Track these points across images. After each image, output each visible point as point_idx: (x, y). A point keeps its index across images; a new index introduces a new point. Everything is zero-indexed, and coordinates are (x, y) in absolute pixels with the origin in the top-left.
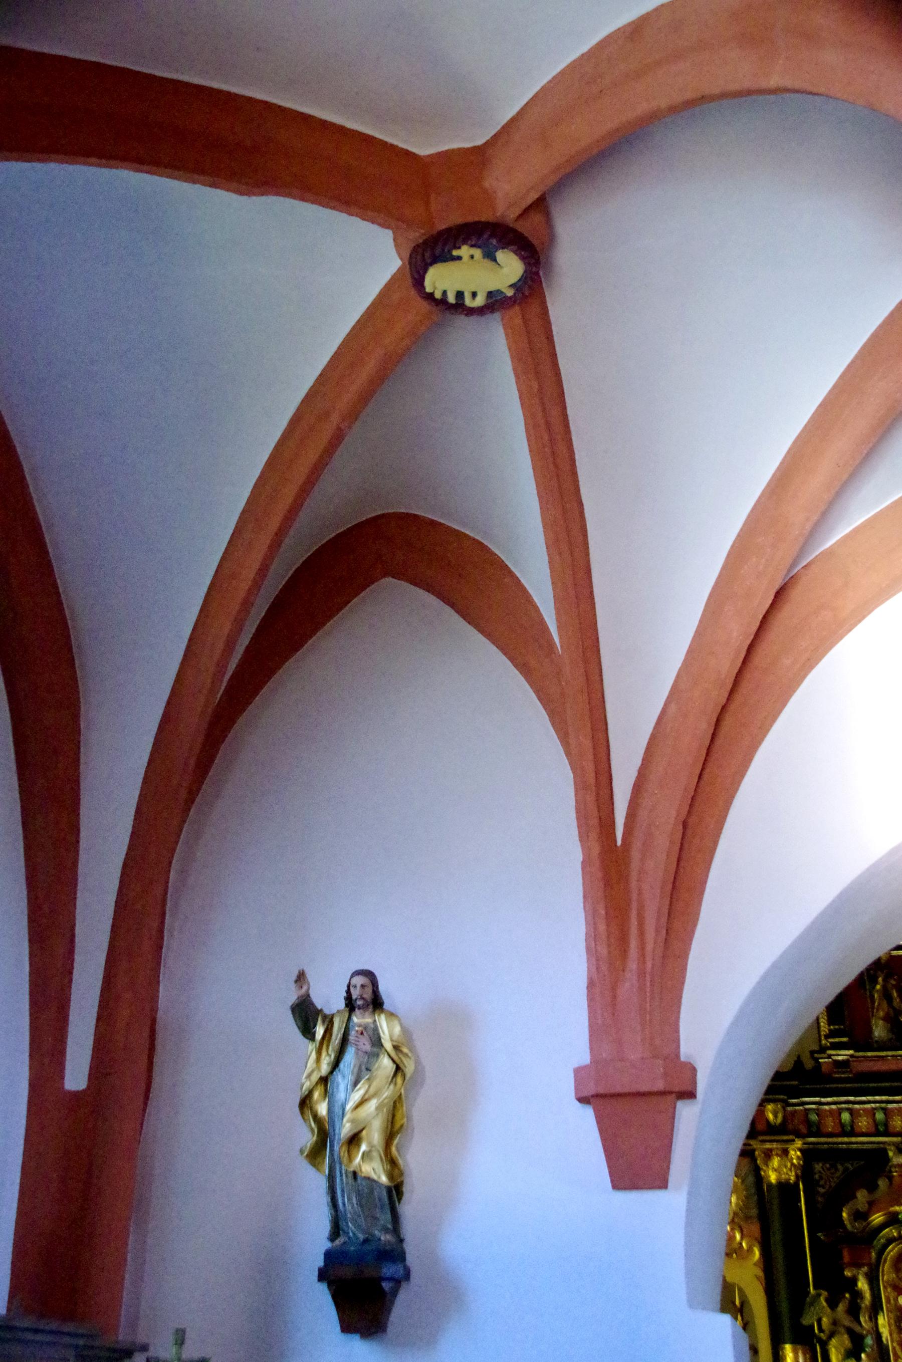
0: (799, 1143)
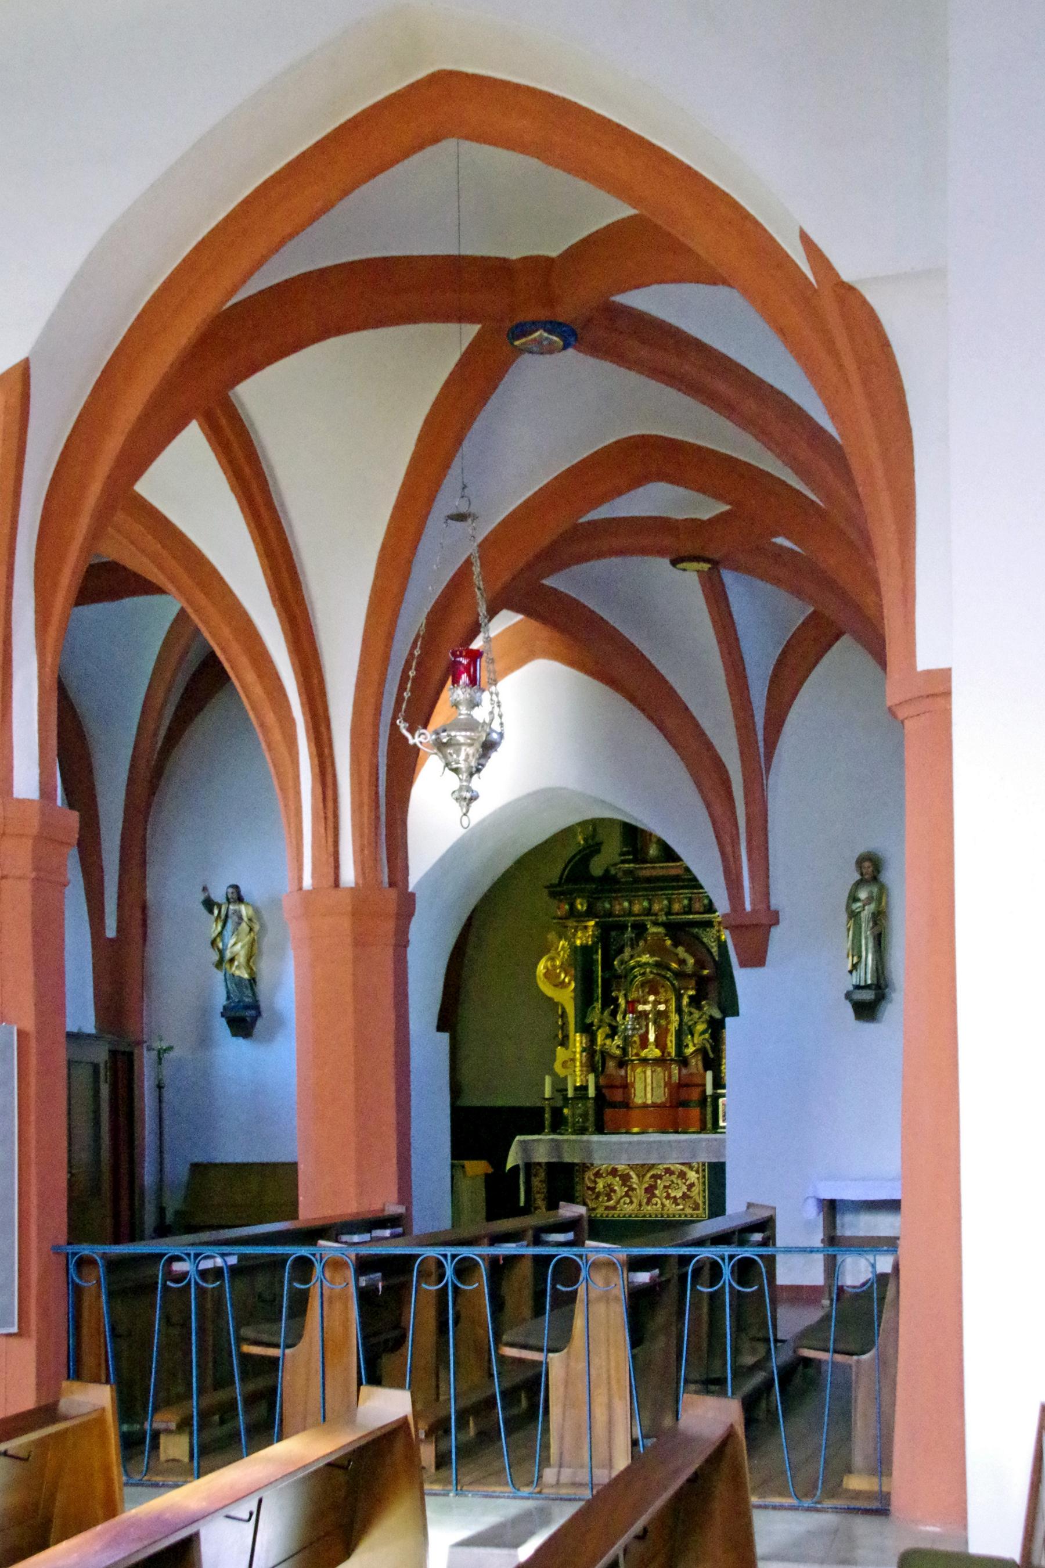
0: (592, 923)
